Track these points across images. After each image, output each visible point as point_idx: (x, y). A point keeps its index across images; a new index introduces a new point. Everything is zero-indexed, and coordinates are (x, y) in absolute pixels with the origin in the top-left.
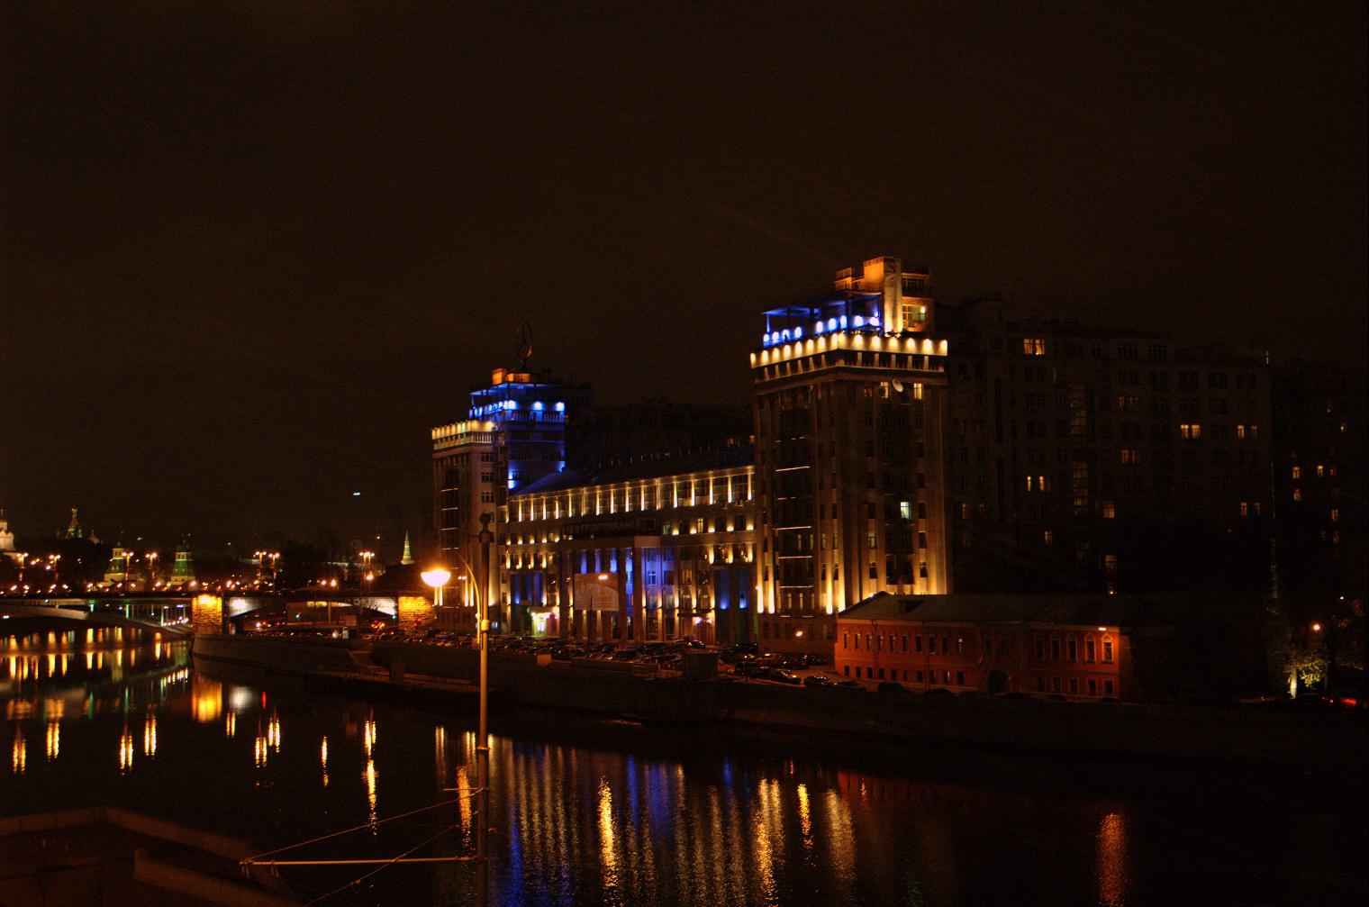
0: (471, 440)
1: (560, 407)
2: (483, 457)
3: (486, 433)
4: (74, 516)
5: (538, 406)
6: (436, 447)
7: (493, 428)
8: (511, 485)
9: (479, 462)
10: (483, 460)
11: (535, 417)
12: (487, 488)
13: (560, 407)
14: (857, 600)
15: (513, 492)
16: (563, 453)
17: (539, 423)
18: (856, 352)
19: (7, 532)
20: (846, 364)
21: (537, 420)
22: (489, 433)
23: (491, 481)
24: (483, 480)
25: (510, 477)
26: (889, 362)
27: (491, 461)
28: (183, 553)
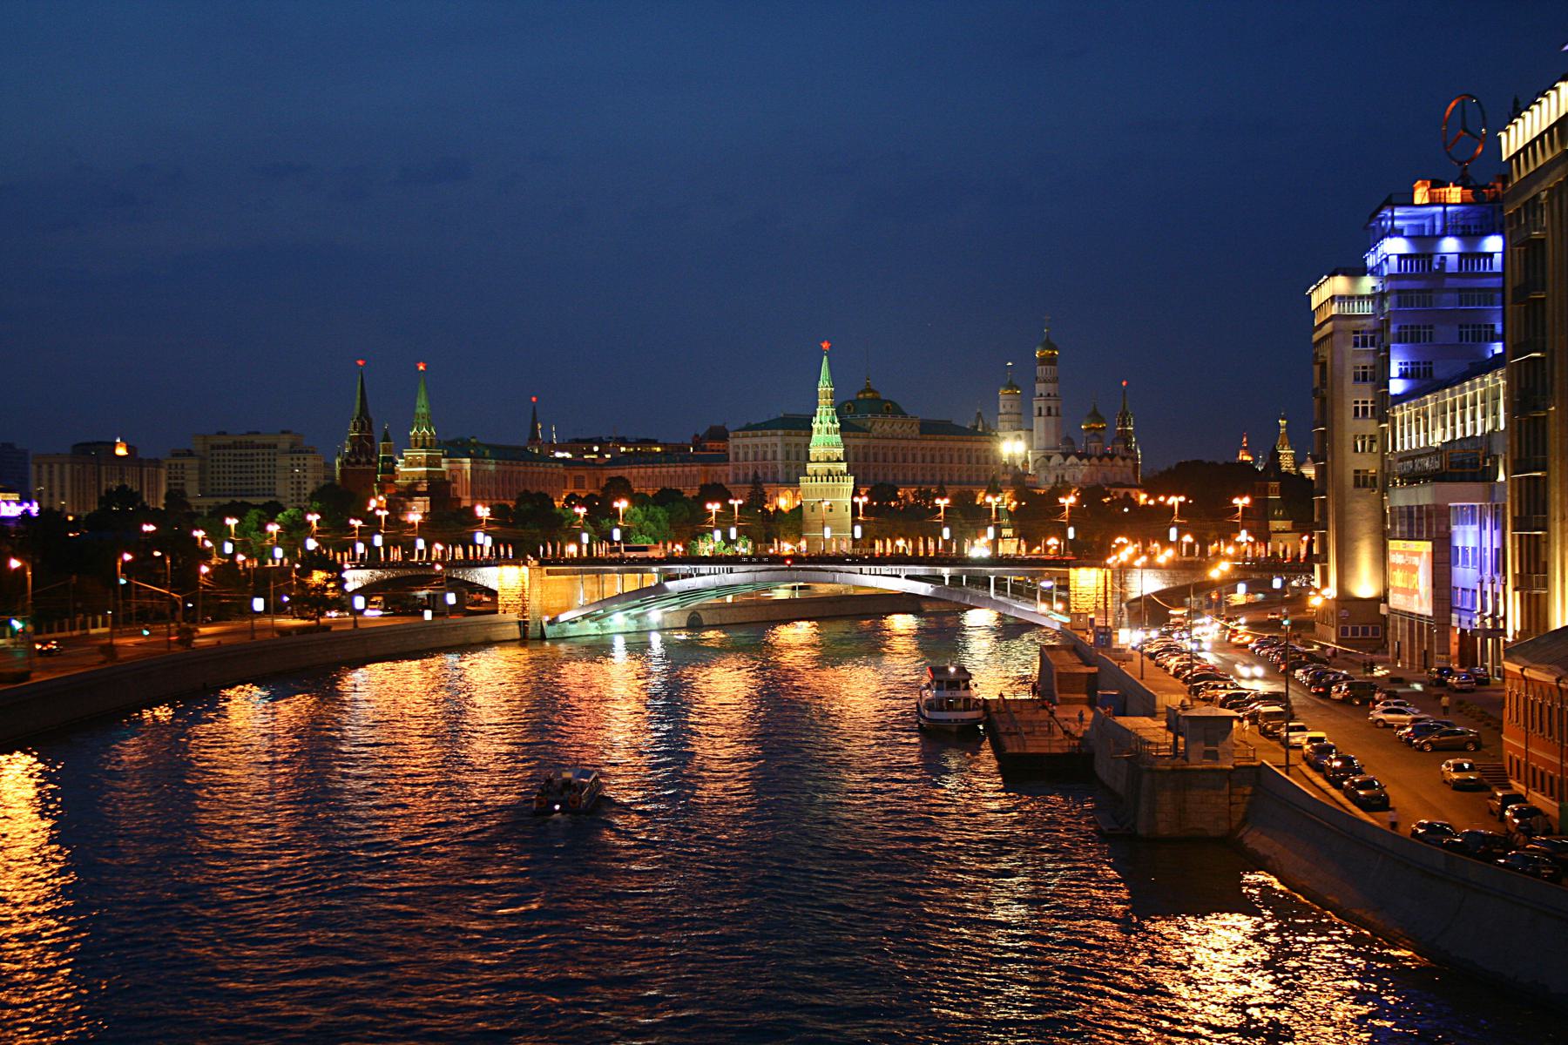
3: (1361, 297)
4: (1282, 430)
5: (1450, 245)
7: (1374, 288)
8: (1397, 386)
9: (1350, 348)
12: (1363, 395)
13: (1493, 244)
15: (1399, 399)
16: (1498, 329)
17: (1451, 275)
21: (1448, 270)
22: (1369, 297)
24: (1356, 379)
25: (1395, 370)
27: (1372, 345)
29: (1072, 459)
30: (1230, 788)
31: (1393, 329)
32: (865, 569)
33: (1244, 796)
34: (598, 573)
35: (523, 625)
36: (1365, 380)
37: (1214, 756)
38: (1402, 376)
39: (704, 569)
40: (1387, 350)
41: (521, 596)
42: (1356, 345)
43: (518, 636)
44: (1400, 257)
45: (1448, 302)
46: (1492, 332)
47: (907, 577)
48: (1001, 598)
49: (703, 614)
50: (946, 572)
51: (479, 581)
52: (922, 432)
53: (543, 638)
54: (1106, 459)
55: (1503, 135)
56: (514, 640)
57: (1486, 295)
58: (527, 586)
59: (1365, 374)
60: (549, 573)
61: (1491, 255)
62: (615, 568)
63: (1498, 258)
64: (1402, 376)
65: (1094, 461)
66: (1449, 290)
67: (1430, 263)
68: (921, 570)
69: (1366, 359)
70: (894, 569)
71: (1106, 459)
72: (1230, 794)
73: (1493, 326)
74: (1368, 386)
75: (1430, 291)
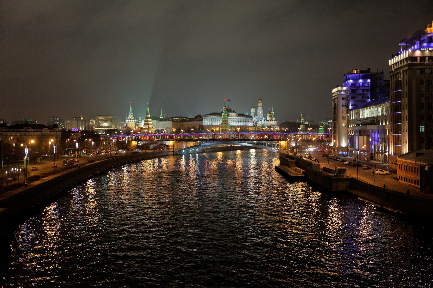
0: (338, 93)
1: (369, 81)
2: (342, 99)
4: (302, 116)
5: (361, 81)
6: (334, 95)
7: (346, 89)
8: (350, 107)
9: (341, 100)
10: (351, 99)
11: (359, 85)
13: (369, 81)
14: (157, 160)
15: (351, 110)
16: (370, 97)
18: (416, 58)
19: (275, 121)
20: (412, 62)
23: (345, 106)
24: (342, 106)
25: (350, 105)
26: (417, 61)
28: (321, 127)
29: (266, 121)
30: (346, 182)
31: (350, 97)
32: (239, 142)
33: (348, 183)
34: (187, 142)
35: (173, 152)
36: (344, 106)
37: (343, 176)
38: (351, 106)
39: (208, 141)
40: (349, 100)
41: (173, 146)
42: (342, 100)
43: (173, 154)
44: (351, 83)
45: (360, 92)
46: (368, 97)
47: (248, 143)
48: (265, 147)
49: (205, 150)
50: (255, 142)
51: (165, 143)
52: (238, 116)
53: (177, 154)
54: (272, 121)
55: (390, 61)
56: (172, 155)
57: (367, 91)
58: (174, 144)
59: (344, 105)
60: (178, 142)
61: (368, 83)
62: (191, 141)
63: (370, 83)
64: (351, 106)
65: (270, 121)
66: (361, 90)
67: (357, 84)
68: (250, 142)
69: (344, 102)
70: (245, 142)
71: (272, 121)
72: (346, 183)
73: (368, 96)
74: (345, 107)
75: (357, 90)
